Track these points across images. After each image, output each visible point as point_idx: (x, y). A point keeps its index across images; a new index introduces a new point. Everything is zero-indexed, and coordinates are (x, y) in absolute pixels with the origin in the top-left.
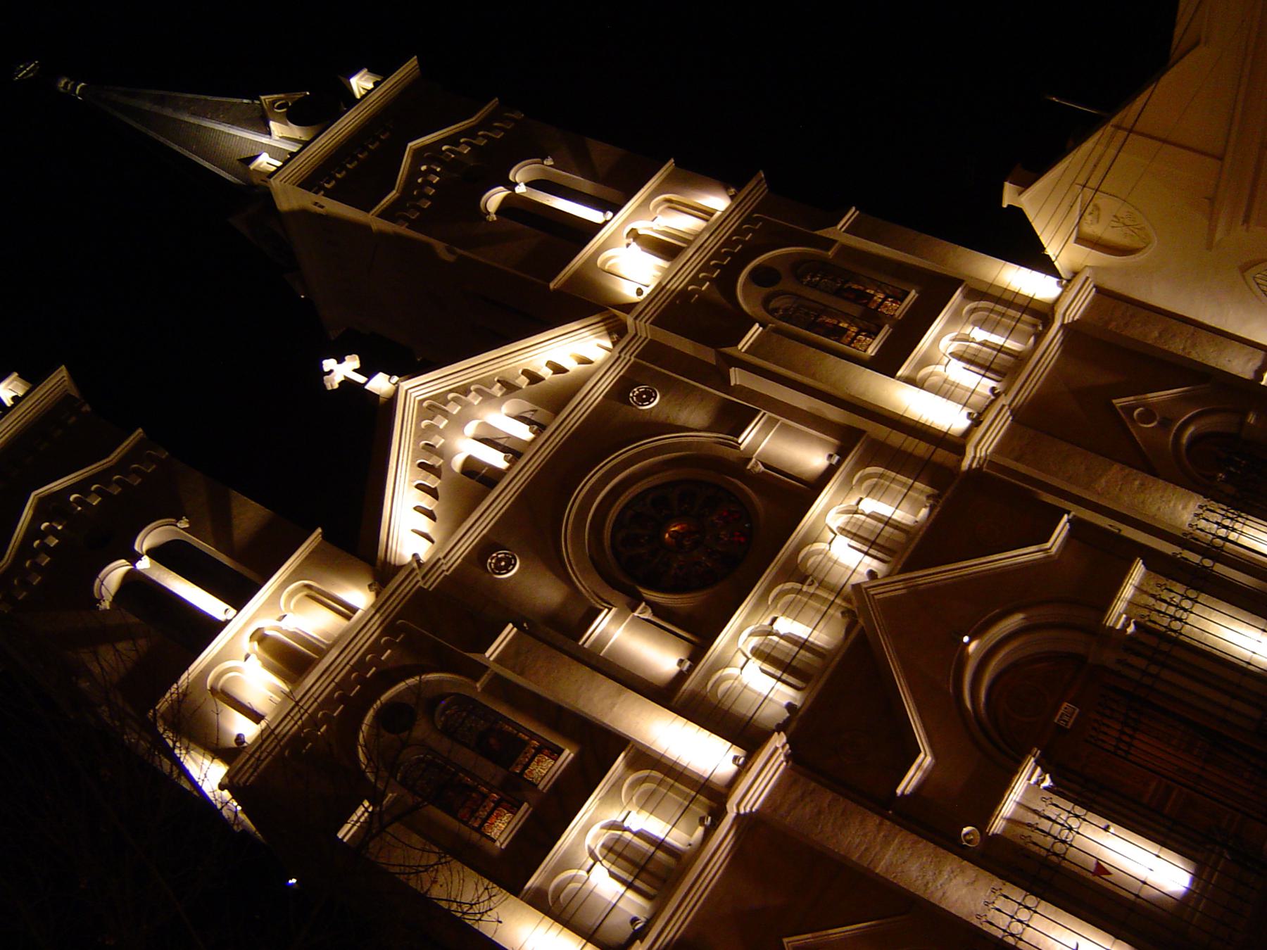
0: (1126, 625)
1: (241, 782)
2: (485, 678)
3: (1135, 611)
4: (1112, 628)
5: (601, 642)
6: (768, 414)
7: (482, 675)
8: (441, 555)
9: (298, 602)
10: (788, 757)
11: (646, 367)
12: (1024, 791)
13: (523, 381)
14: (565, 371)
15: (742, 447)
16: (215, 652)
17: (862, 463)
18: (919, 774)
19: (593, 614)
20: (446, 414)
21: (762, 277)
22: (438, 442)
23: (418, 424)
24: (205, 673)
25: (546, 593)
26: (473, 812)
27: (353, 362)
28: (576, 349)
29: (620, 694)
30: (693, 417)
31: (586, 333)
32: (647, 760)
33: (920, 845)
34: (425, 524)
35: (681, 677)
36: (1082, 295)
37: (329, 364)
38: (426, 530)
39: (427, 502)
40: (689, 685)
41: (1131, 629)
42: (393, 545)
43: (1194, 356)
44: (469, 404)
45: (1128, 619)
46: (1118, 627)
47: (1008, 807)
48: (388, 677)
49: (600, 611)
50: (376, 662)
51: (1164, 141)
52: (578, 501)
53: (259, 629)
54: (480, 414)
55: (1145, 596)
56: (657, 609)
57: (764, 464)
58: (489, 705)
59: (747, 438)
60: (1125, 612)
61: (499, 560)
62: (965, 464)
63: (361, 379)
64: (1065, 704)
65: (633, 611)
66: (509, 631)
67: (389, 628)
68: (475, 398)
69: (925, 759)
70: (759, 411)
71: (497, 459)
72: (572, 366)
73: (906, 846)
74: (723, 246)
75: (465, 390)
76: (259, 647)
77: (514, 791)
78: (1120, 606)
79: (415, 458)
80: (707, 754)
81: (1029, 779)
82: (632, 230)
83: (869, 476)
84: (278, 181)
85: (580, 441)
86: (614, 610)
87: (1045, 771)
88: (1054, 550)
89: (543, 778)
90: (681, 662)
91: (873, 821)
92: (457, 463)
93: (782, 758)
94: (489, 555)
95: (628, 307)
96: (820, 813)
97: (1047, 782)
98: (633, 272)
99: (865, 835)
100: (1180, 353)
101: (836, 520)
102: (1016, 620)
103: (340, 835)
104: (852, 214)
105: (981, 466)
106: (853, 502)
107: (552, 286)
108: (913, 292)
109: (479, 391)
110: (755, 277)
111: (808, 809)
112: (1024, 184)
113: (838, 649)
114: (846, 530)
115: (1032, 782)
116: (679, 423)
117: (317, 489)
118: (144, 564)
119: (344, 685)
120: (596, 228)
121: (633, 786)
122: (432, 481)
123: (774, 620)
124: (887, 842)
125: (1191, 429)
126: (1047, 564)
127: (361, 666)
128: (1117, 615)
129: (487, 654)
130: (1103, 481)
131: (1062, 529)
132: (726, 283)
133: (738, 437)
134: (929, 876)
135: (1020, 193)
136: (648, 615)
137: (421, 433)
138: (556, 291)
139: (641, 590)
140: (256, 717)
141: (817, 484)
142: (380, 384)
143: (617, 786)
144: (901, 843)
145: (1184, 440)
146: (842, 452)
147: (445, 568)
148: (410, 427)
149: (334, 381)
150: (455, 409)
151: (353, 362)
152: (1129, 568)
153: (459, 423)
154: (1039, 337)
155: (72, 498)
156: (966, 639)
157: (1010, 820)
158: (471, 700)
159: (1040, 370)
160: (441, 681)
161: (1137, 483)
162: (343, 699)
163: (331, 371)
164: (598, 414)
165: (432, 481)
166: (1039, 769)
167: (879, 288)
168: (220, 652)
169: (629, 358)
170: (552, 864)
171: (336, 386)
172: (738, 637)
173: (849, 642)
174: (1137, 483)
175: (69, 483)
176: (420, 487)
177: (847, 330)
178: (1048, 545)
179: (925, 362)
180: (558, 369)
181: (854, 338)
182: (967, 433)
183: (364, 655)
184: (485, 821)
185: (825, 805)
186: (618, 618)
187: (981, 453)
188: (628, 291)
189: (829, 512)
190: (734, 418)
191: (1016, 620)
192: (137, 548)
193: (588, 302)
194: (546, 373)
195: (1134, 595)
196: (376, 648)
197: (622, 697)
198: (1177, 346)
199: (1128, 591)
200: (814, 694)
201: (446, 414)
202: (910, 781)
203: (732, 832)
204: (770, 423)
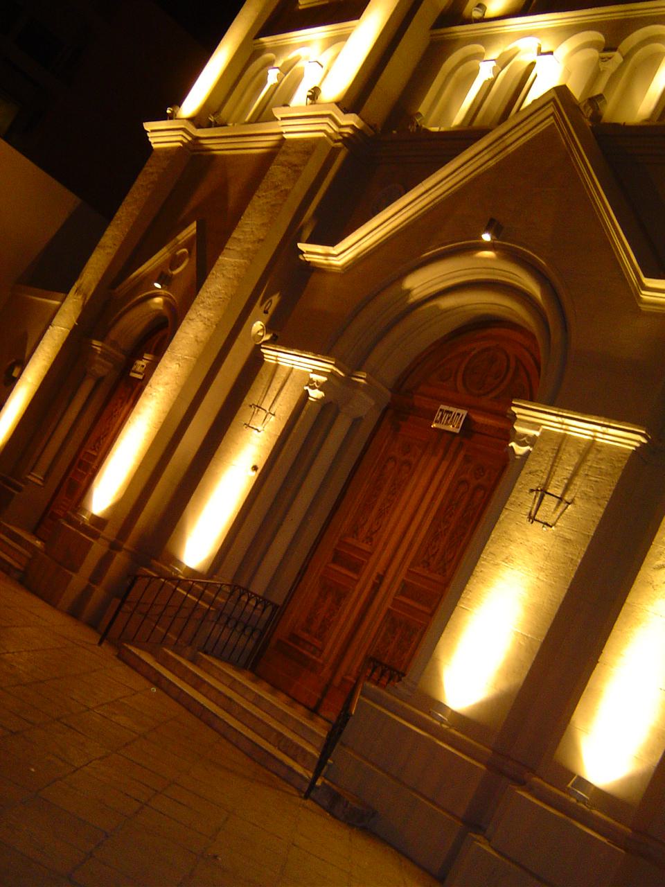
3: (548, 447)
4: (513, 418)
12: (300, 370)
41: (520, 450)
45: (532, 441)
46: (519, 429)
55: (576, 459)
81: (315, 372)
87: (322, 387)
97: (316, 394)
128: (535, 421)
134: (209, 301)
152: (620, 419)
166: (324, 379)
185: (283, 188)
191: (534, 289)
195: (578, 441)
199: (582, 429)
202: (313, 252)
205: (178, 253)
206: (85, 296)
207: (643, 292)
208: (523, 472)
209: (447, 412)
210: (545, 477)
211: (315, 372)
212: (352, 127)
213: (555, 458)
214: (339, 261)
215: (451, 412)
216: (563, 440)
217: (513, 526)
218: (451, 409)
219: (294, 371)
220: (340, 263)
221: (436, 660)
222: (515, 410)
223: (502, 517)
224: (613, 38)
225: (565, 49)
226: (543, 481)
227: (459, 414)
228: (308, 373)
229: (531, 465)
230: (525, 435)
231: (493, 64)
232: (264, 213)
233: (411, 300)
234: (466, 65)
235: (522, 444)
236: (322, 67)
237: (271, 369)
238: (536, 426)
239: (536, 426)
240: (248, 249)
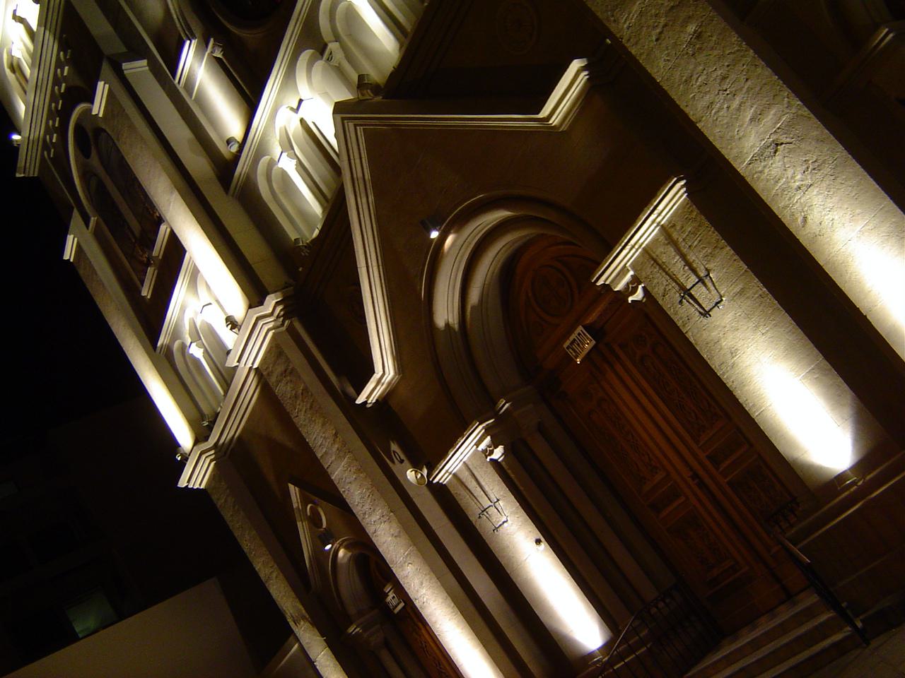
3: (649, 269)
4: (606, 287)
12: (469, 456)
41: (639, 295)
45: (636, 280)
46: (619, 287)
55: (671, 250)
65: (207, 47)
67: (63, 46)
81: (477, 444)
86: (194, 42)
97: (498, 453)
128: (619, 269)
134: (367, 507)
136: (218, 54)
152: (653, 195)
161: (691, 28)
166: (489, 438)
174: (691, 28)
191: (501, 214)
195: (655, 240)
199: (646, 232)
202: (370, 393)
205: (309, 514)
206: (304, 618)
207: (550, 122)
208: (660, 302)
209: (572, 343)
213: (661, 267)
215: (574, 340)
217: (705, 334)
218: (571, 338)
219: (469, 463)
220: (392, 373)
221: (795, 461)
222: (600, 282)
223: (692, 340)
224: (314, 41)
225: (303, 87)
226: (677, 288)
227: (579, 334)
228: (476, 450)
229: (657, 292)
230: (628, 284)
231: (285, 155)
233: (456, 327)
234: (273, 178)
235: (634, 291)
236: (210, 304)
237: (455, 481)
238: (624, 271)
239: (624, 271)
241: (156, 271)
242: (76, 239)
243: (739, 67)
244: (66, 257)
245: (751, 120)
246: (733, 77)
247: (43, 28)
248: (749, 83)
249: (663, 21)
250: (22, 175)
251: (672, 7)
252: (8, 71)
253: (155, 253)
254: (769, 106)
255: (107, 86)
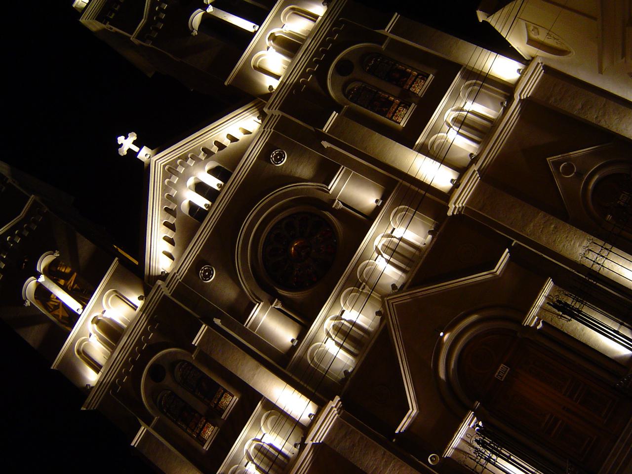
0: (537, 324)
1: (92, 409)
2: (196, 352)
4: (528, 326)
5: (254, 325)
6: (345, 167)
7: (194, 351)
8: (176, 271)
9: (113, 297)
10: (340, 409)
11: (279, 137)
13: (215, 149)
14: (236, 140)
15: (330, 192)
16: (77, 331)
17: (395, 204)
18: (409, 420)
19: (251, 307)
20: (177, 174)
21: (344, 68)
22: (174, 193)
23: (163, 182)
24: (73, 344)
25: (229, 293)
26: (196, 424)
27: (133, 137)
28: (241, 126)
29: (257, 368)
30: (305, 170)
31: (246, 114)
32: (271, 407)
33: (404, 468)
34: (168, 248)
35: (293, 349)
36: (534, 77)
37: (121, 139)
38: (170, 251)
39: (170, 234)
40: (298, 353)
42: (153, 264)
43: (603, 124)
44: (189, 166)
45: (539, 320)
47: (456, 442)
48: (153, 349)
49: (255, 305)
50: (146, 340)
51: (564, 7)
52: (244, 231)
53: (95, 317)
54: (194, 173)
56: (284, 300)
57: (342, 202)
58: (199, 367)
59: (334, 185)
60: (537, 315)
61: (205, 271)
62: (450, 213)
63: (136, 149)
64: (502, 365)
65: (272, 305)
66: (334, 115)
67: (151, 321)
68: (191, 162)
69: (413, 411)
70: (340, 166)
71: (202, 202)
72: (240, 136)
73: (396, 468)
74: (301, 77)
75: (185, 158)
76: (101, 319)
77: (214, 413)
78: (534, 311)
79: (163, 205)
80: (299, 406)
81: (469, 425)
82: (272, 34)
83: (402, 210)
84: (84, 20)
85: (247, 184)
86: (262, 304)
87: (478, 420)
88: (498, 273)
89: (227, 406)
90: (377, 201)
91: (382, 450)
92: (185, 205)
93: (478, 175)
94: (271, 153)
95: (267, 96)
96: (354, 445)
98: (272, 65)
99: (376, 460)
100: (594, 121)
101: (380, 242)
102: (474, 317)
103: (193, 343)
104: (396, 16)
105: (460, 212)
106: (389, 232)
107: (226, 83)
108: (431, 75)
109: (193, 158)
110: (339, 69)
111: (348, 444)
112: (490, 12)
113: (376, 331)
114: (389, 243)
115: (471, 426)
116: (297, 175)
117: (108, 241)
118: (42, 279)
119: (133, 354)
120: (250, 36)
121: (267, 418)
122: (172, 220)
123: (343, 312)
124: (386, 465)
125: (596, 177)
126: (496, 279)
127: (139, 343)
128: (532, 318)
129: (324, 130)
130: (532, 225)
131: (506, 255)
132: (321, 76)
133: (328, 185)
135: (488, 17)
137: (165, 189)
138: (229, 86)
139: (277, 289)
140: (97, 367)
141: (370, 217)
142: (144, 154)
143: (258, 420)
144: (394, 466)
145: (591, 187)
146: (384, 198)
147: (179, 277)
148: (159, 185)
149: (123, 151)
150: (181, 170)
151: (133, 137)
153: (184, 178)
154: (506, 110)
155: (8, 240)
156: (442, 334)
157: (456, 449)
158: (189, 364)
159: (503, 136)
160: (176, 352)
161: (553, 226)
162: (133, 361)
163: (122, 144)
164: (255, 170)
165: (172, 220)
166: (475, 418)
167: (413, 69)
168: (78, 332)
169: (270, 130)
170: (229, 461)
171: (125, 153)
172: (324, 322)
173: (433, 243)
174: (553, 226)
175: (7, 229)
176: (166, 224)
177: (411, 73)
178: (495, 270)
179: (435, 130)
180: (233, 139)
181: (397, 109)
182: (452, 191)
183: (140, 337)
184: (202, 429)
186: (264, 309)
187: (459, 205)
188: (269, 83)
189: (376, 237)
190: (326, 173)
191: (474, 317)
192: (38, 269)
193: (243, 95)
194: (227, 142)
195: (544, 303)
196: (145, 333)
197: (259, 370)
198: (592, 117)
199: (541, 301)
200: (363, 359)
201: (177, 174)
202: (404, 425)
203: (311, 452)
204: (347, 174)
208: (551, 323)
209: (499, 373)
210: (554, 315)
211: (469, 425)
212: (339, 401)
214: (413, 410)
215: (500, 371)
216: (542, 308)
217: (571, 328)
218: (498, 371)
219: (466, 439)
220: (415, 411)
222: (525, 325)
226: (556, 316)
227: (502, 368)
228: (469, 428)
230: (536, 323)
232: (367, 452)
235: (539, 323)
237: (463, 444)
238: (534, 317)
239: (534, 317)
240: (385, 461)
241: (219, 429)
242: (146, 429)
243: (571, 233)
244: (132, 444)
245: (579, 246)
246: (570, 236)
247: (142, 313)
248: (575, 236)
249: (542, 226)
250: (85, 409)
251: (545, 222)
252: (76, 353)
253: (223, 417)
254: (584, 240)
255: (207, 327)
